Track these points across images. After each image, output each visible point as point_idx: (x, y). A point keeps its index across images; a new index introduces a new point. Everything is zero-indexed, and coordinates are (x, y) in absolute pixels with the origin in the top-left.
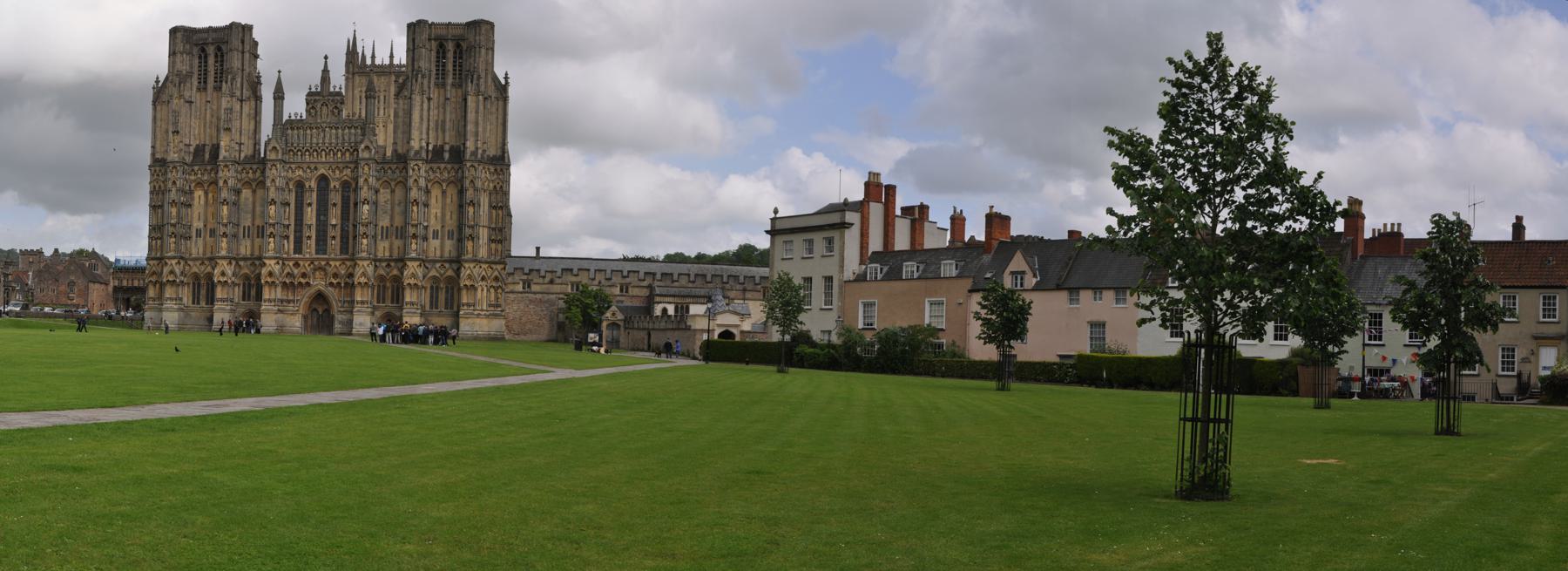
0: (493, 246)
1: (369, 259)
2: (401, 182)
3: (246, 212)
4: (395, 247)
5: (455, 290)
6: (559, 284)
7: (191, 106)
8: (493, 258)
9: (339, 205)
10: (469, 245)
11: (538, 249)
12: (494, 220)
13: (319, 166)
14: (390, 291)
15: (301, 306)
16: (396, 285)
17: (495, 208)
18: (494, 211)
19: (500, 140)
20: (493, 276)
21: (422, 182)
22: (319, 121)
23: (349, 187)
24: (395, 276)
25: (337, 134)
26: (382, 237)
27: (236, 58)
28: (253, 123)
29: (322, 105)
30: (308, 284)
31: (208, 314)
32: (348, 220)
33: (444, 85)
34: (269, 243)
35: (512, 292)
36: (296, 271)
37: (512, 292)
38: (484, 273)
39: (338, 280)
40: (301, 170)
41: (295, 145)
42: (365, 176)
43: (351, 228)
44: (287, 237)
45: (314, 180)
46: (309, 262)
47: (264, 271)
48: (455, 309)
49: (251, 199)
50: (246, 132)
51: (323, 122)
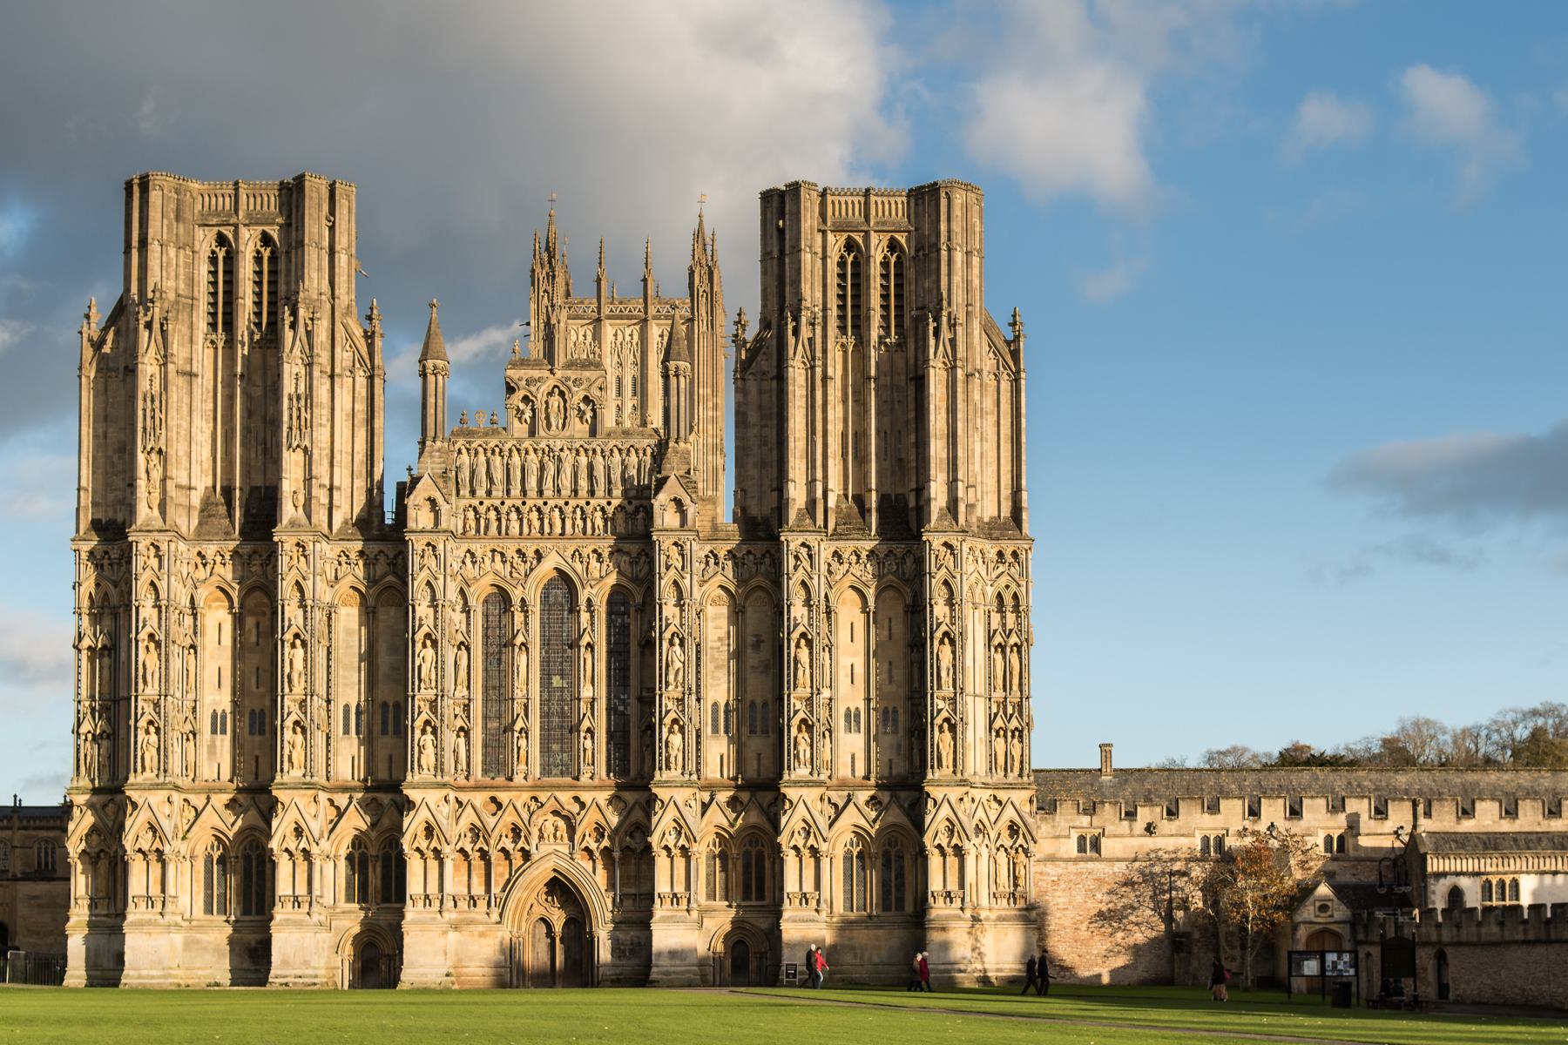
1: (689, 784)
4: (751, 755)
5: (908, 862)
6: (1172, 835)
10: (943, 741)
11: (1106, 750)
12: (1000, 682)
14: (740, 864)
15: (508, 913)
16: (753, 851)
23: (625, 603)
24: (754, 827)
25: (591, 467)
26: (715, 730)
27: (314, 264)
28: (361, 435)
29: (550, 394)
30: (526, 855)
31: (252, 938)
35: (1052, 859)
36: (491, 821)
37: (1052, 859)
38: (980, 813)
39: (606, 843)
40: (498, 558)
41: (481, 492)
43: (633, 709)
44: (465, 732)
46: (526, 796)
47: (413, 824)
48: (909, 907)
50: (347, 459)
51: (555, 437)
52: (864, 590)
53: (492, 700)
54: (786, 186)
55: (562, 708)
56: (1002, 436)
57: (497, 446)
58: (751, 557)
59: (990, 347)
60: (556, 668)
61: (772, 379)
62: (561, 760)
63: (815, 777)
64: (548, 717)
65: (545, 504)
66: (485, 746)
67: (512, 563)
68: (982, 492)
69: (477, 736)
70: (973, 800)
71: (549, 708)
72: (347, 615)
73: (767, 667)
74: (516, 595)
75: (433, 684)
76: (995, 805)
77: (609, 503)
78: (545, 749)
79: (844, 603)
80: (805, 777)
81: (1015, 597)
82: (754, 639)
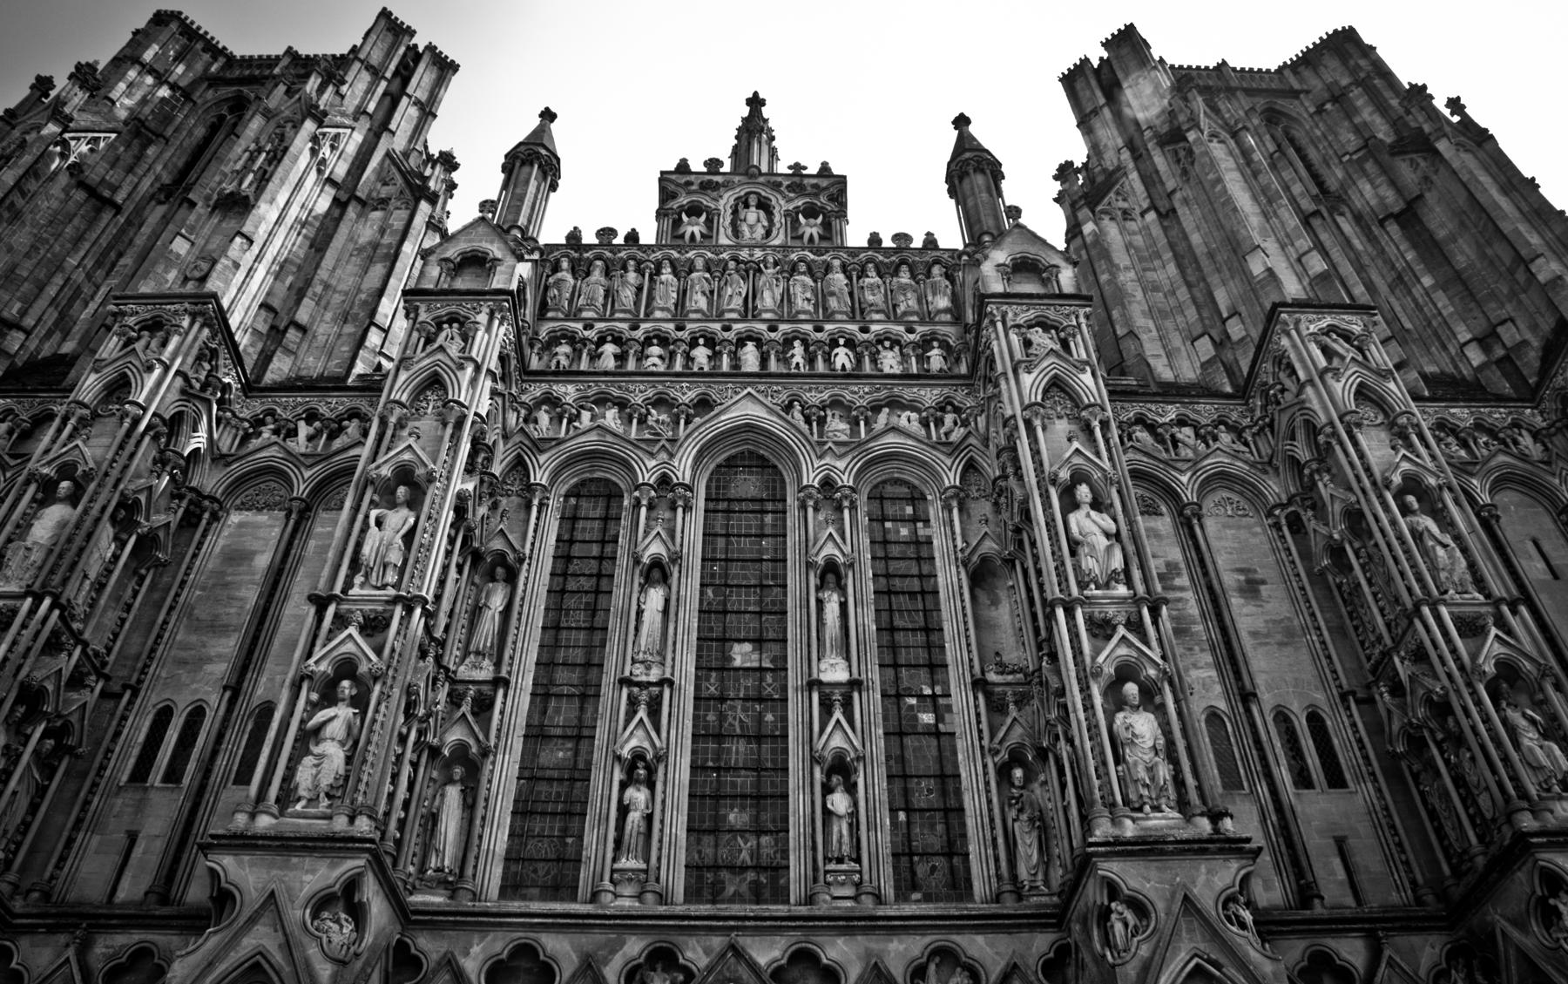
2: (1222, 478)
3: (217, 628)
4: (1315, 841)
7: (98, 211)
9: (862, 582)
23: (917, 498)
32: (936, 667)
34: (310, 736)
42: (1049, 366)
46: (635, 947)
49: (263, 561)
53: (559, 696)
54: (1106, 45)
55: (760, 718)
58: (1188, 431)
61: (1143, 214)
62: (756, 853)
64: (719, 737)
65: (727, 329)
66: (523, 810)
69: (503, 775)
72: (241, 525)
73: (1290, 633)
74: (648, 470)
75: (391, 577)
77: (865, 330)
82: (1242, 578)
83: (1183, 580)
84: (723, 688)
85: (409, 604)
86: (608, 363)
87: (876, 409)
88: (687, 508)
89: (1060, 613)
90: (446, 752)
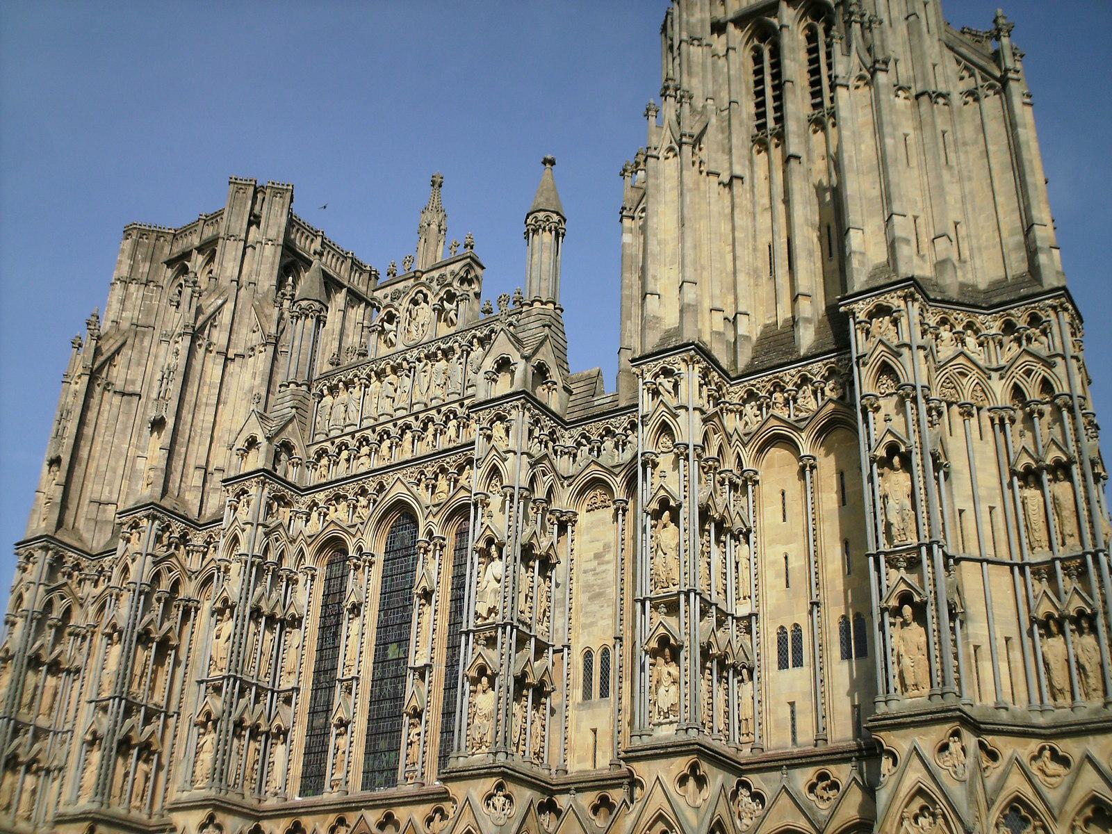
0: (1054, 648)
7: (129, 403)
8: (1062, 712)
12: (1041, 535)
13: (388, 479)
17: (1031, 477)
18: (1032, 494)
19: (1011, 220)
20: (1080, 794)
21: (690, 429)
22: (400, 347)
26: (587, 695)
33: (781, 136)
44: (283, 734)
45: (371, 525)
46: (332, 818)
51: (416, 346)
52: (794, 435)
56: (995, 167)
57: (356, 376)
59: (959, 63)
60: (393, 634)
62: (387, 763)
63: (682, 737)
67: (355, 507)
68: (971, 250)
70: (993, 756)
71: (381, 690)
76: (1053, 767)
78: (371, 752)
79: (769, 466)
80: (667, 738)
81: (1046, 386)
83: (610, 557)
84: (384, 672)
85: (229, 678)
86: (343, 464)
87: (461, 469)
88: (371, 564)
89: (463, 638)
90: (274, 731)
